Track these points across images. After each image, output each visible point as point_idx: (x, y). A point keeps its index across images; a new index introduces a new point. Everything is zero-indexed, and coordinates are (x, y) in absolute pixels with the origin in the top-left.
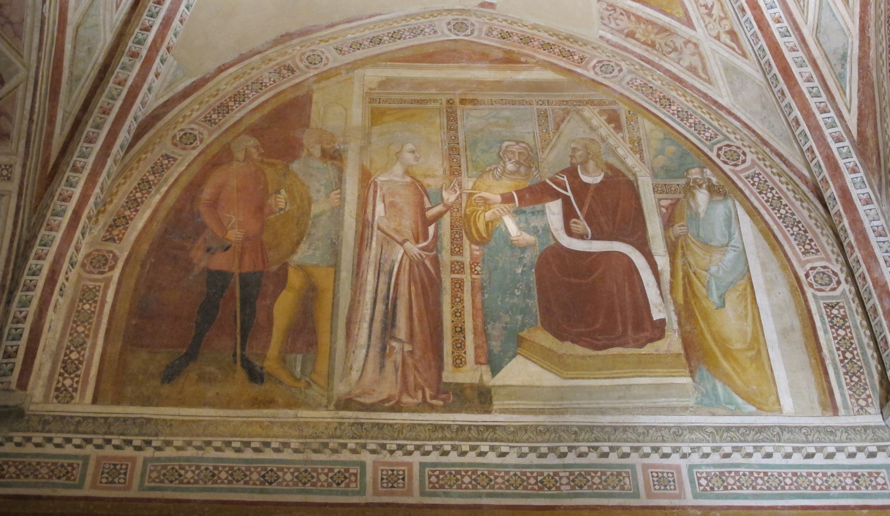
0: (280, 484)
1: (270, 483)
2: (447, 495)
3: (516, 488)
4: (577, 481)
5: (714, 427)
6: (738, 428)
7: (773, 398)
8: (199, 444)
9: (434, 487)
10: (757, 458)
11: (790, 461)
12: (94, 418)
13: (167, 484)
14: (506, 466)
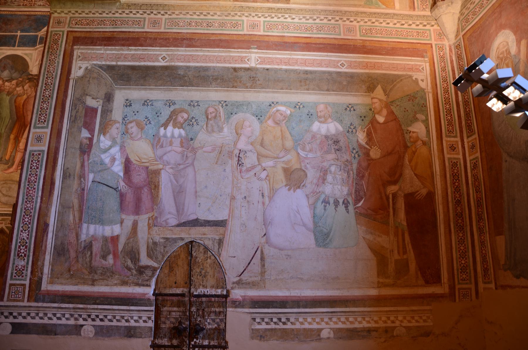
0: (214, 27)
1: (210, 27)
2: (272, 32)
3: (297, 30)
4: (319, 29)
5: (370, 13)
6: (378, 13)
7: (392, 4)
8: (184, 13)
9: (268, 29)
10: (384, 24)
11: (396, 26)
12: (146, 4)
13: (174, 27)
14: (294, 23)
